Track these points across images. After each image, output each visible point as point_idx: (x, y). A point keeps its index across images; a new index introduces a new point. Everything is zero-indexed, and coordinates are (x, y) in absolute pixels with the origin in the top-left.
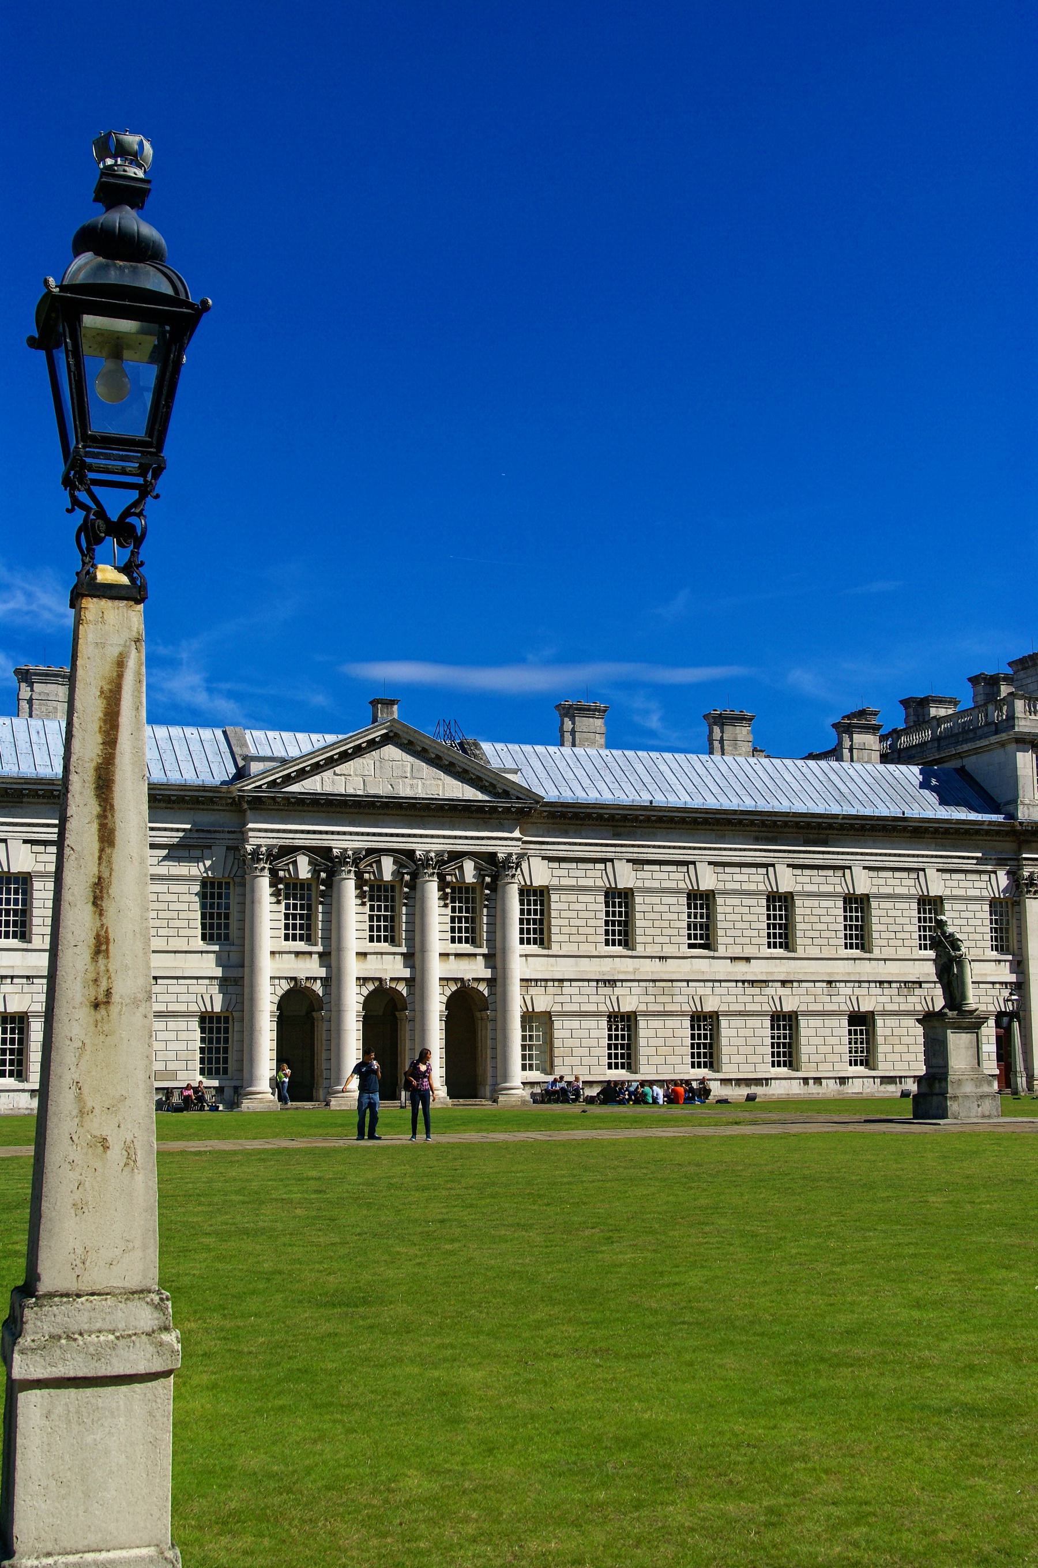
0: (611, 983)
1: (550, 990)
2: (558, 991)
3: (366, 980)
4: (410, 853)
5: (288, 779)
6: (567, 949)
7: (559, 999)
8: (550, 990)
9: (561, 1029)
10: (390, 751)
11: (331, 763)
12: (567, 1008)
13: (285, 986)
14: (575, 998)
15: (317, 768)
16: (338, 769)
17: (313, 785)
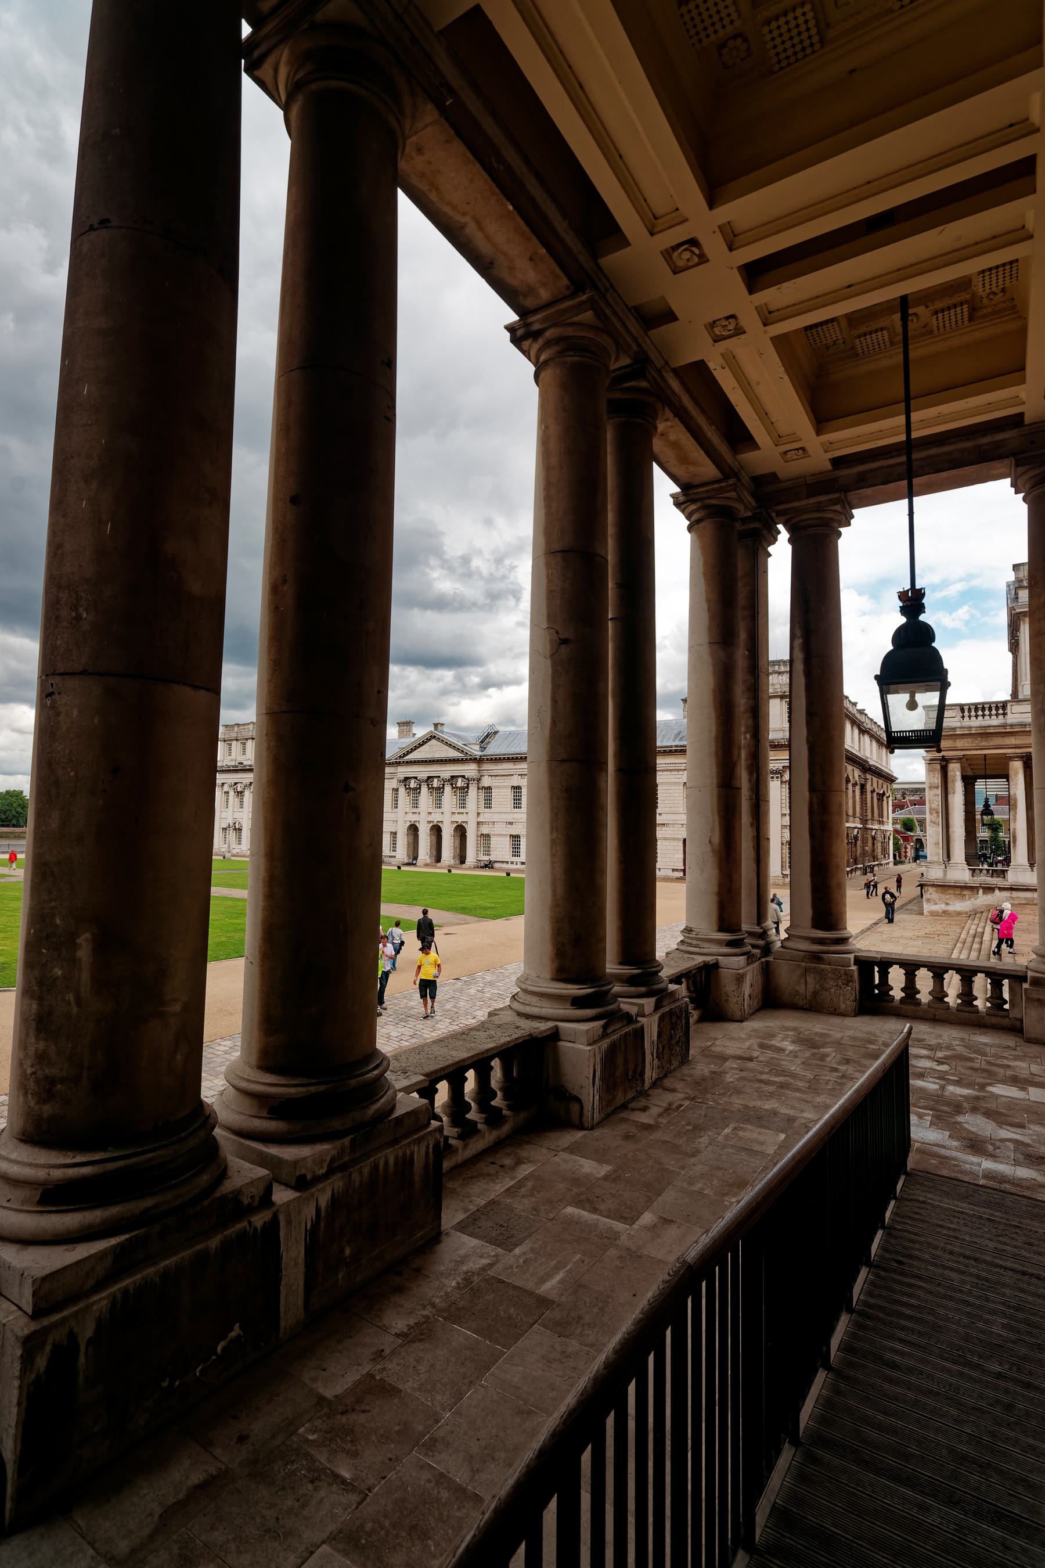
0: (511, 823)
1: (490, 826)
2: (493, 826)
3: (431, 822)
4: (439, 777)
5: (405, 755)
6: (497, 810)
7: (493, 829)
8: (490, 826)
9: (494, 840)
10: (433, 741)
11: (416, 748)
12: (496, 833)
13: (408, 824)
14: (500, 829)
15: (412, 750)
16: (418, 750)
17: (411, 757)
